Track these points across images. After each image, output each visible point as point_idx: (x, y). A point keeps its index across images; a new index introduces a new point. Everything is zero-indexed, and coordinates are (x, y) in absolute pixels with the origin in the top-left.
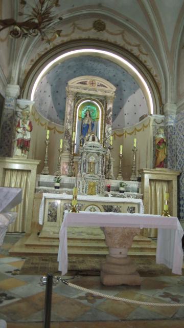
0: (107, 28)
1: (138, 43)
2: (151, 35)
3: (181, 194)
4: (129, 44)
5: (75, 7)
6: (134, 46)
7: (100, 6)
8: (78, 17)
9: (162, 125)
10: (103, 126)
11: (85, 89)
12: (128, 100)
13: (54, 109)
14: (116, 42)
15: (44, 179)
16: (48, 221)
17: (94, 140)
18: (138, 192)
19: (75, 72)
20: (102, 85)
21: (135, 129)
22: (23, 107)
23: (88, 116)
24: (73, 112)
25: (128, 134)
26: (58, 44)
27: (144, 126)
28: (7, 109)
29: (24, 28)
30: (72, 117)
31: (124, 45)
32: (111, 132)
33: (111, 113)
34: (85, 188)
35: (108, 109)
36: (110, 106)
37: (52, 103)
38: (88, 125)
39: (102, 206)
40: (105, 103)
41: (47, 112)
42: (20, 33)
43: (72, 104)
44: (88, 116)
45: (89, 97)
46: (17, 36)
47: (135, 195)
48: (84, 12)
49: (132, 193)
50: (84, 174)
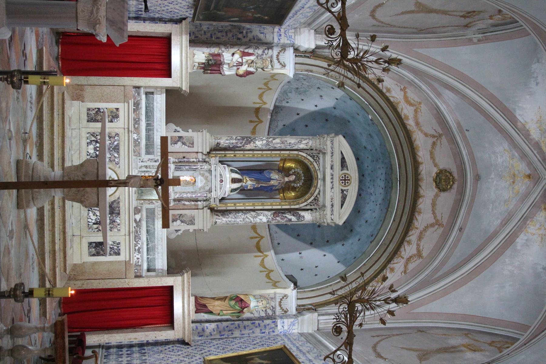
0: (443, 194)
1: (424, 254)
2: (440, 273)
3: (150, 347)
4: (420, 238)
5: (467, 133)
6: (418, 245)
7: (477, 178)
8: (453, 141)
9: (278, 311)
10: (270, 207)
11: (332, 168)
13: (296, 117)
14: (420, 213)
15: (159, 100)
16: (89, 109)
17: (234, 181)
18: (149, 270)
19: (365, 148)
21: (272, 271)
22: (280, 57)
24: (288, 147)
25: (263, 260)
26: (399, 110)
27: (276, 282)
28: (273, 33)
29: (340, 40)
30: (278, 146)
31: (417, 228)
32: (258, 220)
33: (294, 219)
34: (149, 170)
35: (302, 213)
36: (308, 217)
37: (306, 113)
38: (270, 179)
39: (119, 198)
40: (312, 207)
41: (288, 105)
42: (332, 36)
43: (302, 146)
46: (327, 33)
47: (142, 261)
48: (464, 152)
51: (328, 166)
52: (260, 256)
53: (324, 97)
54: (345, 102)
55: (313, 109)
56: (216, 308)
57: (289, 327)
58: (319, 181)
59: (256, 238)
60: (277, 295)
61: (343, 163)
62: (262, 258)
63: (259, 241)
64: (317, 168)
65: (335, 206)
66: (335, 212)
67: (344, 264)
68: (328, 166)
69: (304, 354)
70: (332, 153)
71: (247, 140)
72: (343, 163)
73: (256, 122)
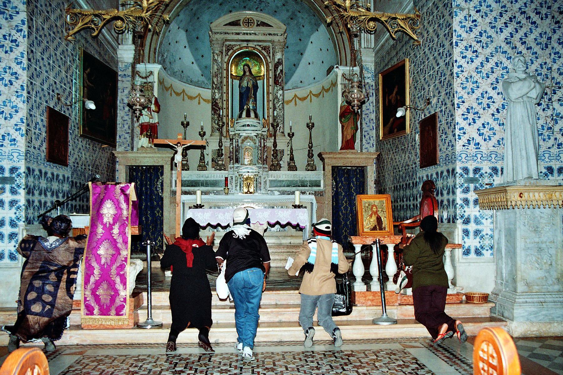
11: (238, 34)
12: (311, 41)
13: (195, 64)
17: (248, 115)
20: (264, 24)
23: (248, 74)
33: (280, 68)
38: (248, 88)
43: (219, 60)
44: (248, 74)
45: (245, 44)
49: (310, 188)
50: (236, 165)
51: (237, 37)
53: (178, 40)
54: (181, 21)
55: (188, 50)
58: (249, 45)
59: (295, 100)
60: (343, 82)
61: (235, 23)
63: (299, 98)
64: (238, 47)
65: (271, 32)
66: (276, 33)
67: (319, 26)
68: (237, 37)
69: (391, 59)
70: (226, 33)
71: (215, 105)
72: (235, 23)
73: (199, 100)
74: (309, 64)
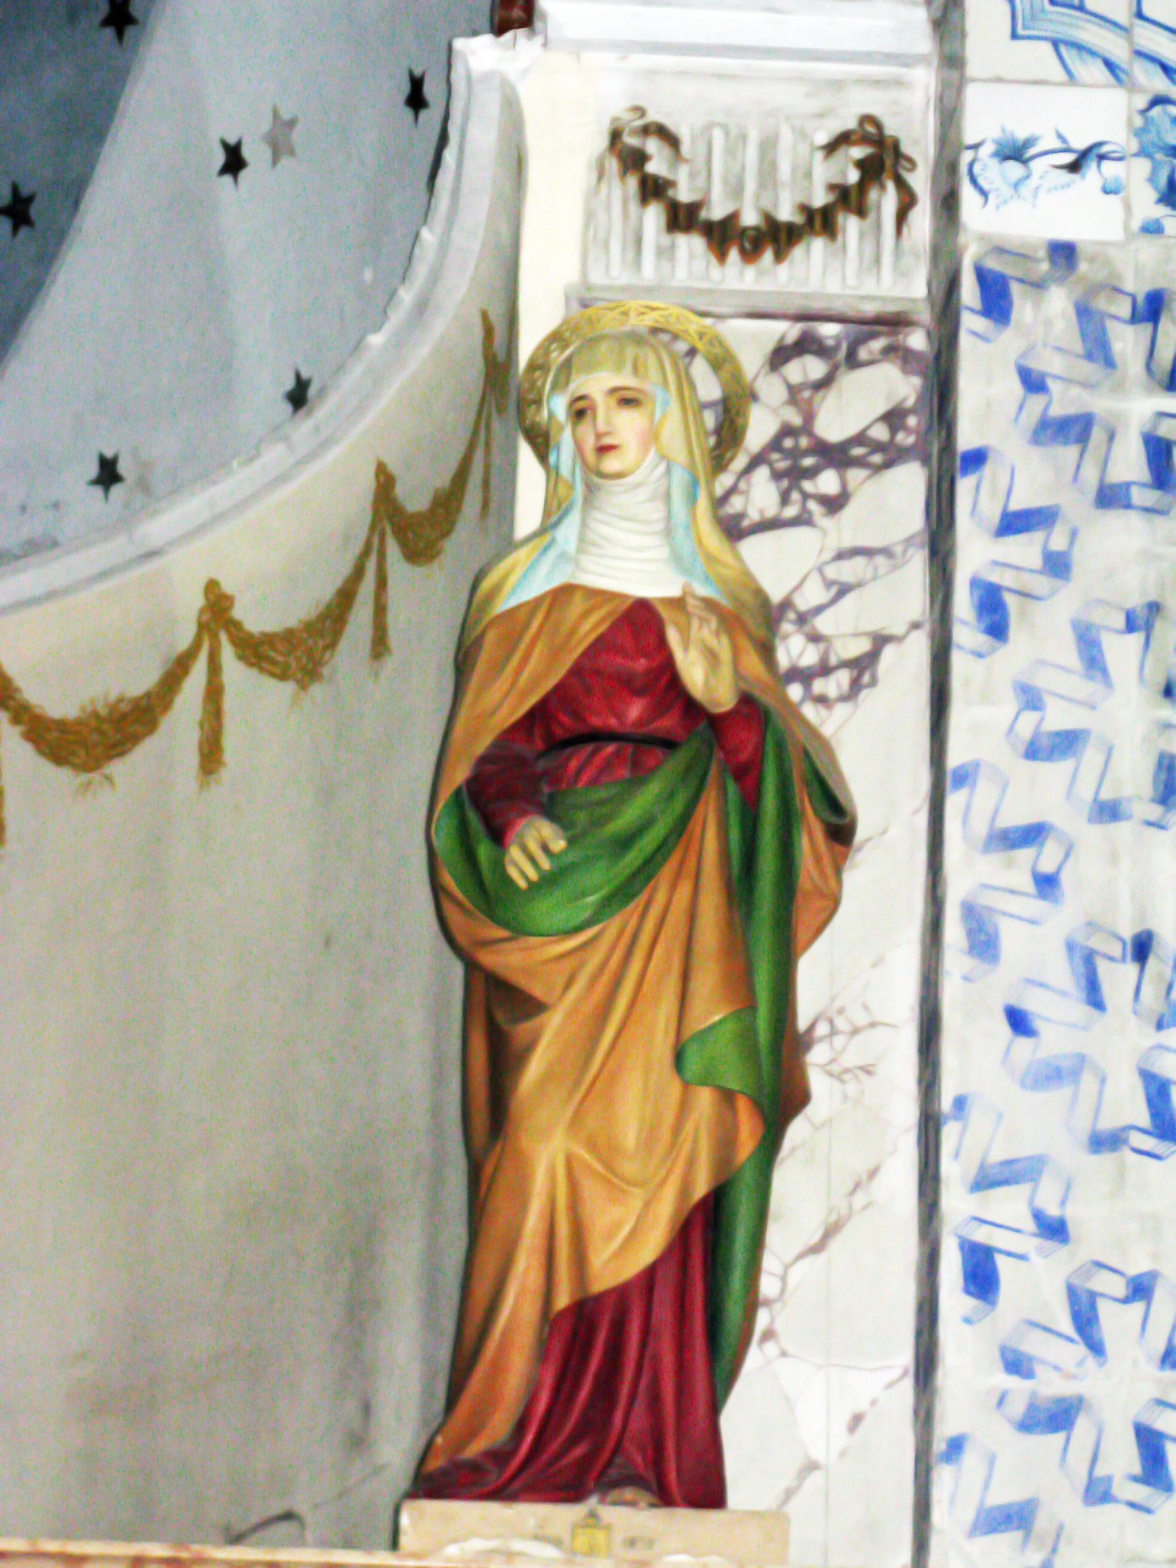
52: (214, 692)
56: (630, 1138)
57: (1095, 71)
62: (233, 668)
74: (234, 162)
